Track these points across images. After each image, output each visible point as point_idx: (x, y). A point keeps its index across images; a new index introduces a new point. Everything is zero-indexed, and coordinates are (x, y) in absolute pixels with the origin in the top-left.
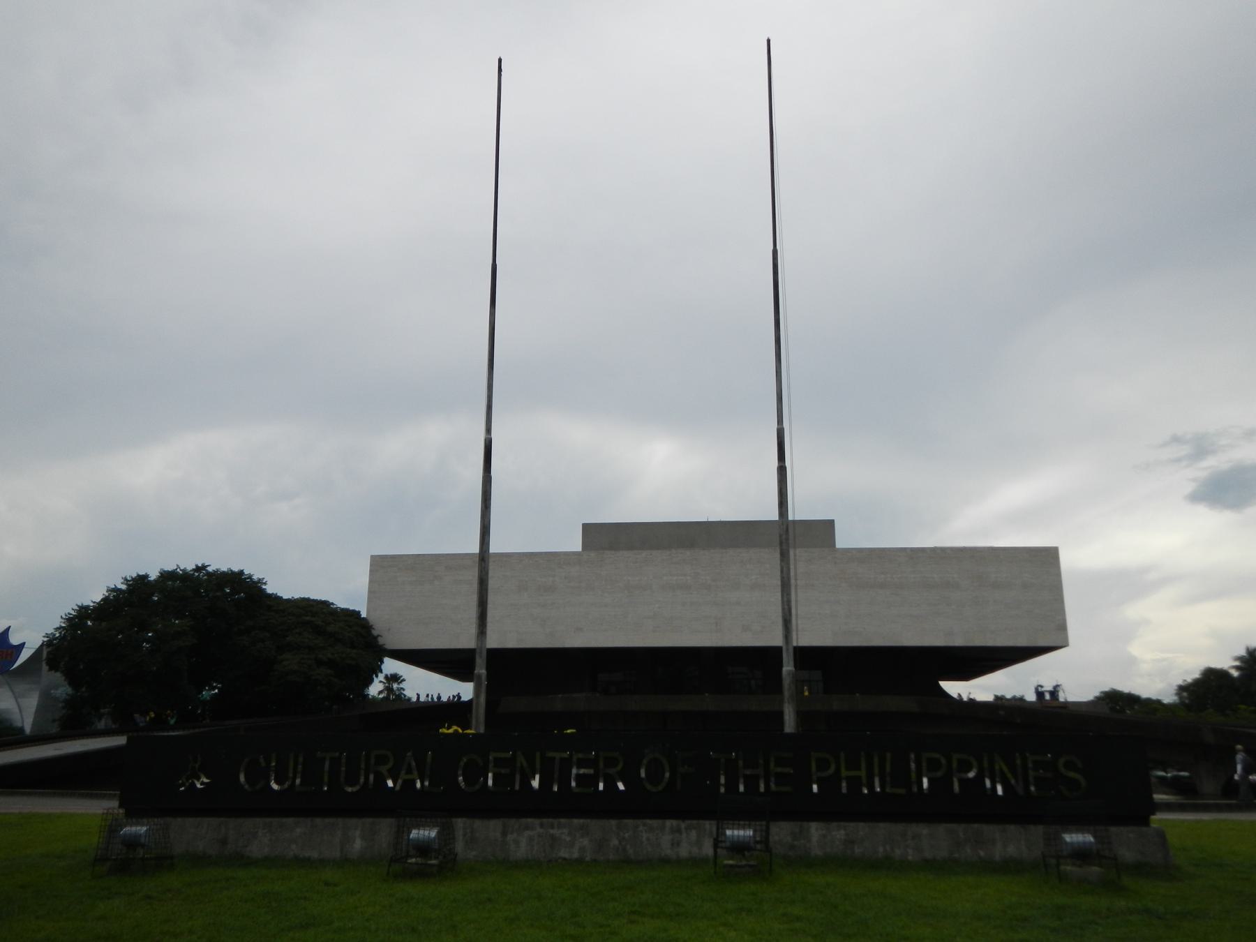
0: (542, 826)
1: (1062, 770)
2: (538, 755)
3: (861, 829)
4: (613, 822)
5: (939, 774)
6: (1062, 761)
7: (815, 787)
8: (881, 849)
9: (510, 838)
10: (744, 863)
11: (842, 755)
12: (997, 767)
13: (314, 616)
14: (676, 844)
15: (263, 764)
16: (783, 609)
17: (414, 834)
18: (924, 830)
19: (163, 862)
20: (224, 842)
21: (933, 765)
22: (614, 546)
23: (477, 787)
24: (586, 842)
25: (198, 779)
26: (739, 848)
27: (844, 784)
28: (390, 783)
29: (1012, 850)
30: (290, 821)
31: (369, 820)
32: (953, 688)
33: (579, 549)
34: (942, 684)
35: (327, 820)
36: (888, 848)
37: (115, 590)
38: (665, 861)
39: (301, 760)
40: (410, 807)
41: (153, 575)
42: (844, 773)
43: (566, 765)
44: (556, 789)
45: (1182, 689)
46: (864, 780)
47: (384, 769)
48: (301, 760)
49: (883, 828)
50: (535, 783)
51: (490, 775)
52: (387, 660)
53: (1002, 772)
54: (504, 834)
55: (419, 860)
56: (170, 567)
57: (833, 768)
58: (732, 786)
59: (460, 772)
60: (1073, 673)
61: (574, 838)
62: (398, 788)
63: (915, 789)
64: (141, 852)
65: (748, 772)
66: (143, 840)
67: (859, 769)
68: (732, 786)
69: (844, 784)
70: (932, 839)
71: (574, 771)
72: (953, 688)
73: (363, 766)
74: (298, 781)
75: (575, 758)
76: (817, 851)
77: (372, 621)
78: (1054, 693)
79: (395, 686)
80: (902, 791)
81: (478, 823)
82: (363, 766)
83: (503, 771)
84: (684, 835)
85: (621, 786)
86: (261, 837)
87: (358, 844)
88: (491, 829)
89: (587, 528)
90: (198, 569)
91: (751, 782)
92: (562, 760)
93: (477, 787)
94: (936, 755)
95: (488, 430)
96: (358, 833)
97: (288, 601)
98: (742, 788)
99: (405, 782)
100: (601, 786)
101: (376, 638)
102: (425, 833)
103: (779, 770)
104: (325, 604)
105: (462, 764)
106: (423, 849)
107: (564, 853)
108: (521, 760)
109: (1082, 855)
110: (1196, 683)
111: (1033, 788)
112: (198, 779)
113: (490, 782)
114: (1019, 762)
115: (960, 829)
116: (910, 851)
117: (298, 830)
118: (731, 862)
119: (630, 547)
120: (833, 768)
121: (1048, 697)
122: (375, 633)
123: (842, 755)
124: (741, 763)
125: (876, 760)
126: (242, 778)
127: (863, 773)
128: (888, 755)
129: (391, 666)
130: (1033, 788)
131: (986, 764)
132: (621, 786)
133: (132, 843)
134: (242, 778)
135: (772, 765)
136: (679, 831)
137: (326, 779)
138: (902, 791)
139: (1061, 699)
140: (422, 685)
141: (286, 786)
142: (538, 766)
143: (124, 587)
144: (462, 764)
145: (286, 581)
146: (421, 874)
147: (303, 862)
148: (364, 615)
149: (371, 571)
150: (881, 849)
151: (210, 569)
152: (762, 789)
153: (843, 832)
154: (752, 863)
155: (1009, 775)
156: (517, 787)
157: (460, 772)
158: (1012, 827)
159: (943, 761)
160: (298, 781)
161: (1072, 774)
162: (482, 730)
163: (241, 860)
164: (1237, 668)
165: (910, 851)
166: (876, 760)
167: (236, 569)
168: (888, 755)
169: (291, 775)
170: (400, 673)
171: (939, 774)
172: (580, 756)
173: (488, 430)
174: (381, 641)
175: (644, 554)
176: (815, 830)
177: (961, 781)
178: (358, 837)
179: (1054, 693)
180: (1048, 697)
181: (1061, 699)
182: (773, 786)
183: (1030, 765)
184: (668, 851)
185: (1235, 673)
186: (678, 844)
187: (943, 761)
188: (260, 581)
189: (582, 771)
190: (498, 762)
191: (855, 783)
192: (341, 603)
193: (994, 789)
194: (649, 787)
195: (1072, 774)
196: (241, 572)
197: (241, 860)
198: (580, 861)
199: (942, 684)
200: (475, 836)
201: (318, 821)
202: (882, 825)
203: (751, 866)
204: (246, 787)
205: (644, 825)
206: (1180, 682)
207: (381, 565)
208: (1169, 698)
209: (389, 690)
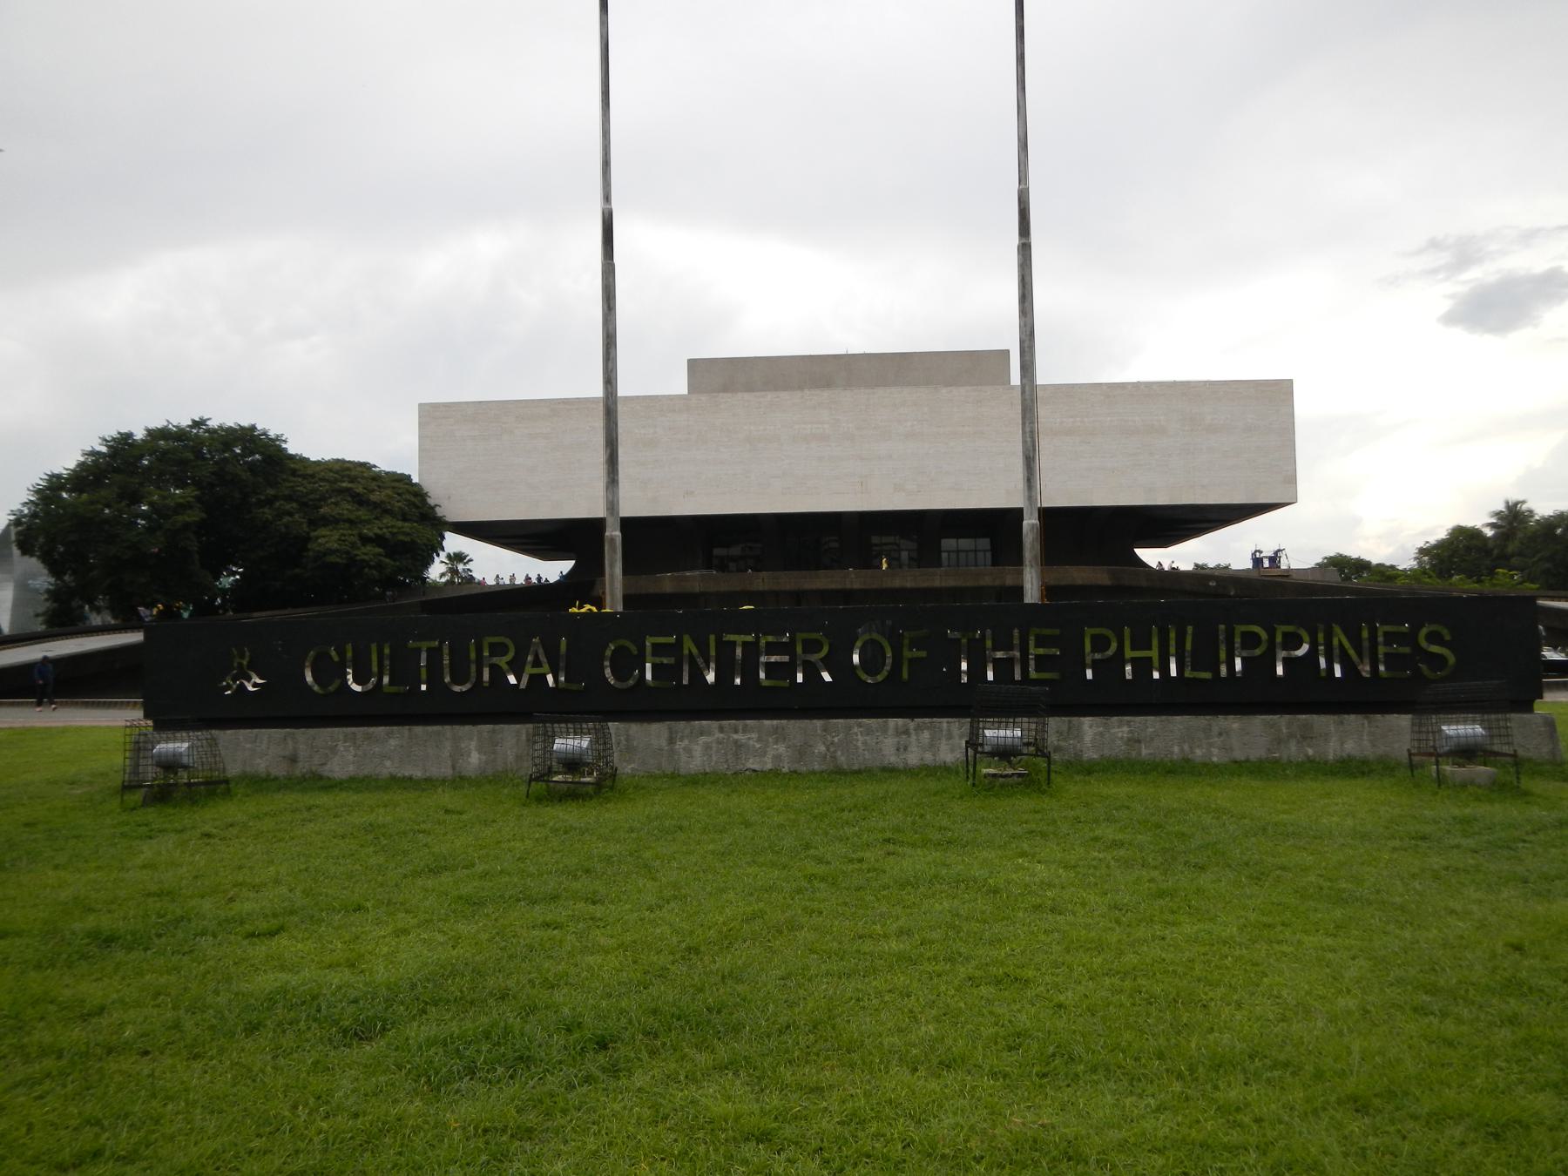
0: (721, 729)
1: (1424, 644)
2: (712, 638)
3: (1150, 724)
4: (818, 723)
5: (1258, 652)
6: (1424, 631)
7: (1089, 674)
8: (1176, 749)
9: (679, 745)
10: (1010, 771)
11: (1127, 630)
12: (1335, 642)
13: (352, 483)
14: (902, 749)
15: (336, 659)
16: (1024, 442)
17: (559, 744)
18: (1233, 723)
19: (216, 787)
20: (293, 760)
21: (1250, 640)
22: (728, 387)
23: (631, 682)
24: (781, 748)
25: (249, 679)
26: (1004, 753)
27: (1128, 668)
28: (512, 680)
29: (1350, 747)
30: (380, 730)
31: (486, 728)
33: (685, 391)
34: (1138, 551)
35: (430, 728)
36: (1186, 747)
37: (93, 453)
38: (890, 771)
39: (387, 651)
40: (532, 708)
41: (139, 435)
42: (1129, 654)
43: (752, 650)
44: (738, 681)
45: (1422, 551)
46: (1156, 662)
47: (502, 661)
48: (387, 651)
49: (1180, 722)
50: (711, 677)
51: (648, 665)
52: (448, 535)
53: (1341, 644)
54: (671, 741)
55: (569, 778)
56: (158, 423)
57: (1114, 645)
58: (977, 672)
59: (607, 663)
60: (1297, 537)
61: (765, 743)
62: (523, 686)
63: (1224, 670)
64: (183, 777)
65: (999, 655)
66: (185, 760)
67: (1149, 648)
68: (977, 672)
69: (1128, 668)
70: (1247, 735)
71: (763, 659)
73: (473, 655)
74: (386, 680)
75: (763, 642)
76: (1090, 754)
77: (427, 487)
78: (1274, 559)
79: (461, 567)
80: (1207, 675)
81: (635, 729)
82: (473, 655)
83: (665, 661)
84: (914, 737)
85: (827, 677)
86: (342, 751)
87: (475, 759)
88: (651, 736)
89: (693, 364)
90: (197, 424)
91: (1003, 668)
92: (745, 644)
93: (631, 682)
94: (1256, 629)
95: (607, 198)
96: (473, 744)
97: (318, 463)
98: (990, 676)
99: (532, 677)
100: (800, 678)
101: (432, 508)
102: (569, 743)
103: (1041, 651)
104: (365, 466)
105: (608, 653)
106: (572, 764)
107: (752, 764)
108: (689, 646)
109: (1467, 753)
110: (1441, 545)
111: (1382, 668)
112: (249, 679)
113: (649, 676)
114: (1365, 634)
115: (1282, 721)
116: (1215, 751)
117: (393, 742)
118: (991, 771)
119: (749, 388)
120: (1114, 645)
121: (1266, 564)
122: (431, 502)
123: (1127, 630)
124: (989, 643)
125: (1173, 635)
126: (309, 678)
127: (1154, 654)
128: (1190, 629)
129: (454, 542)
130: (1382, 668)
131: (1321, 637)
132: (827, 677)
133: (170, 765)
134: (309, 678)
135: (1032, 643)
136: (907, 732)
137: (424, 675)
138: (1207, 675)
139: (1283, 567)
140: (496, 566)
141: (370, 686)
142: (713, 653)
143: (104, 449)
144: (608, 653)
145: (314, 438)
146: (573, 795)
147: (407, 783)
148: (415, 480)
149: (420, 424)
150: (1176, 749)
151: (213, 424)
152: (1018, 677)
153: (1125, 729)
154: (1021, 770)
155: (1352, 652)
156: (685, 682)
157: (607, 663)
158: (1353, 717)
159: (1264, 635)
160: (386, 680)
161: (1435, 649)
162: (620, 609)
163: (318, 782)
164: (1492, 525)
165: (1215, 751)
166: (1173, 635)
167: (245, 423)
168: (1190, 629)
169: (375, 669)
170: (465, 551)
171: (1258, 652)
172: (770, 639)
173: (607, 198)
174: (440, 512)
175: (770, 396)
176: (1089, 726)
177: (1286, 662)
178: (471, 748)
179: (1274, 559)
180: (1266, 564)
181: (1283, 567)
182: (1033, 674)
183: (1381, 639)
184: (892, 759)
185: (1489, 533)
186: (906, 749)
187: (1264, 635)
188: (278, 438)
189: (773, 659)
190: (658, 650)
191: (1143, 667)
193: (1330, 669)
194: (864, 676)
195: (1435, 649)
196: (253, 428)
197: (318, 782)
198: (775, 773)
199: (1138, 551)
200: (642, 743)
201: (418, 730)
202: (1178, 718)
203: (1020, 775)
204: (316, 688)
205: (860, 725)
206: (1421, 544)
207: (433, 416)
208: (1406, 562)
209: (454, 572)
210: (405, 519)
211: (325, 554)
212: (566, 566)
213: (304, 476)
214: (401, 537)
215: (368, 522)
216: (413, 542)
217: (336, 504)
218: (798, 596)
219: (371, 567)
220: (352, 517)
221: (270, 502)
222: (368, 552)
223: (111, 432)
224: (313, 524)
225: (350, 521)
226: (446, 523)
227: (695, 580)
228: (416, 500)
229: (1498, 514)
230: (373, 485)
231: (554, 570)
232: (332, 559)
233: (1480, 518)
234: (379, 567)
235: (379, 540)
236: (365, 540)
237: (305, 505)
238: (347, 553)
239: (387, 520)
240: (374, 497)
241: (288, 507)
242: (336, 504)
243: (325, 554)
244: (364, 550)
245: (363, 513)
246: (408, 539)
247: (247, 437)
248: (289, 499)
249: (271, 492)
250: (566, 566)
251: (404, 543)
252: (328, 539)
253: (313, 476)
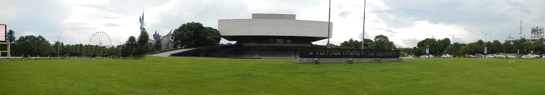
13: (210, 29)
32: (314, 43)
72: (314, 43)
106: (350, 61)
208: (339, 45)
218: (270, 47)
222: (213, 39)
224: (207, 35)
227: (253, 44)
229: (351, 40)
231: (234, 43)
233: (348, 40)
235: (215, 38)
252: (209, 38)
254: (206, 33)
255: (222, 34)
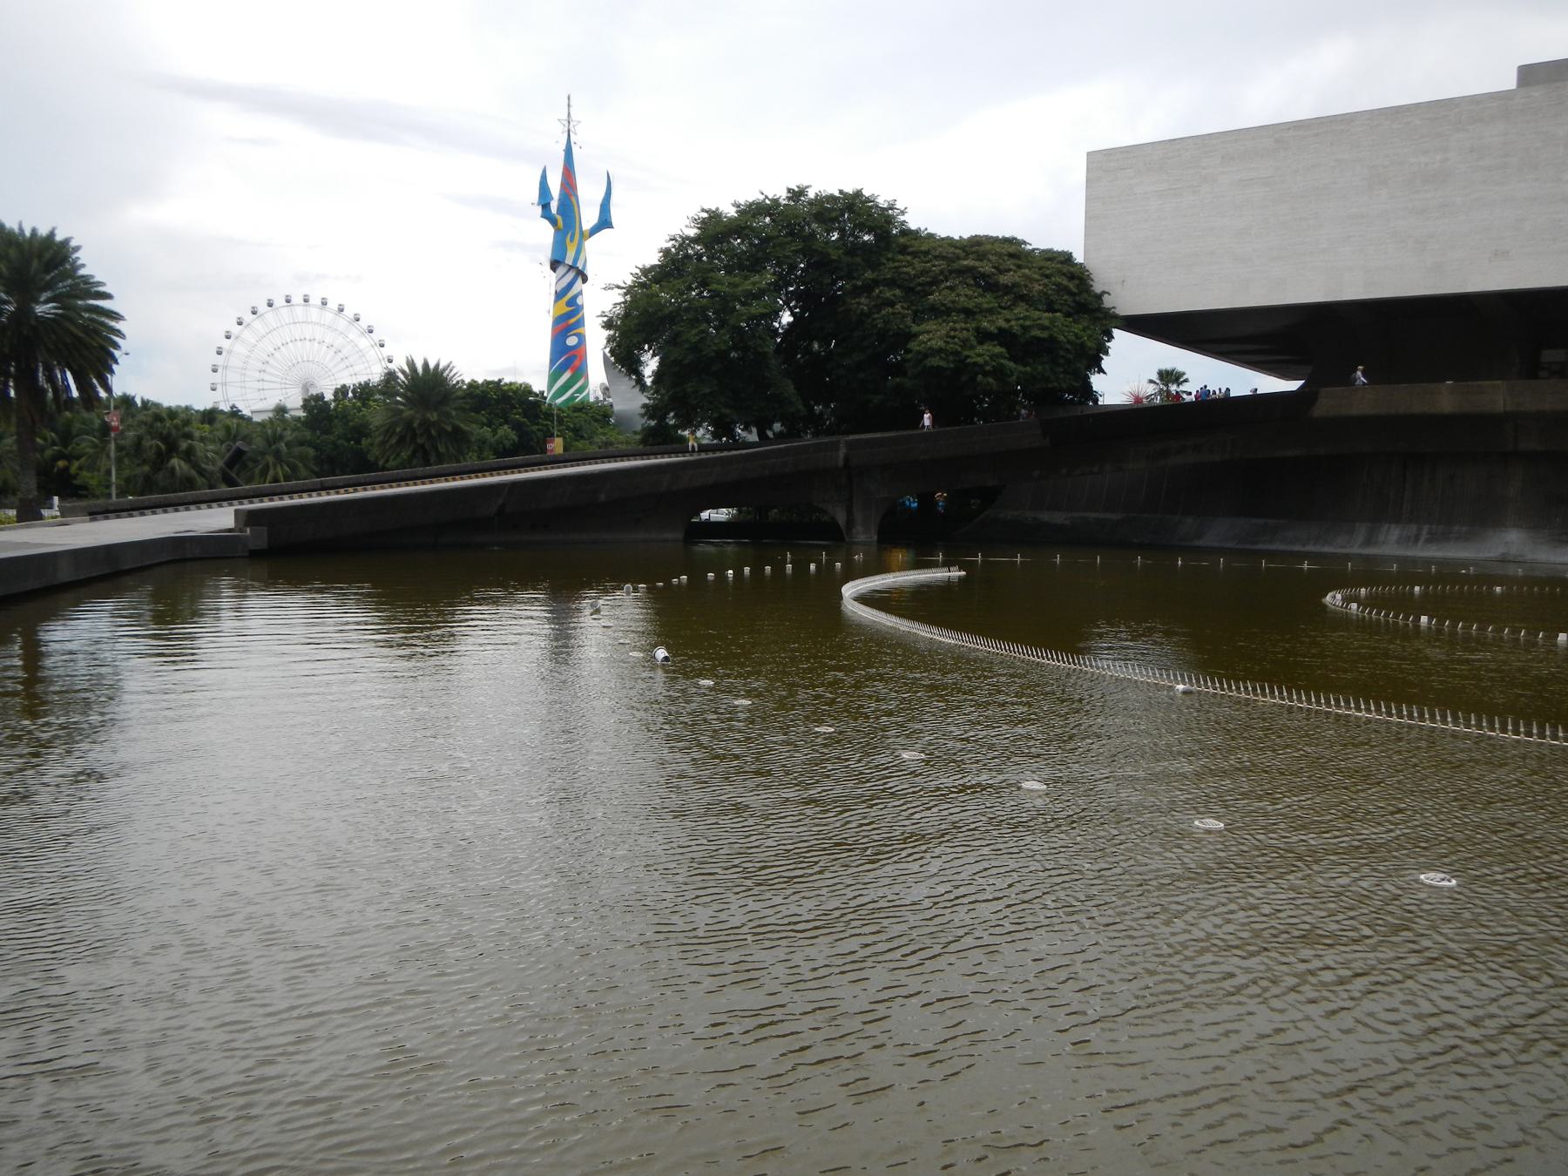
13: (992, 266)
52: (1116, 332)
56: (750, 195)
79: (1173, 388)
90: (797, 194)
122: (1097, 288)
148: (1079, 258)
167: (849, 190)
174: (1108, 302)
192: (1038, 240)
196: (858, 194)
210: (1050, 308)
211: (926, 356)
212: (1300, 383)
213: (915, 254)
214: (1036, 333)
215: (990, 311)
216: (1052, 339)
217: (951, 288)
219: (986, 374)
220: (971, 305)
221: (868, 288)
222: (983, 353)
223: (695, 211)
224: (917, 318)
225: (968, 313)
226: (1116, 317)
228: (1072, 286)
230: (1010, 263)
232: (934, 361)
234: (999, 373)
235: (1003, 337)
236: (984, 336)
237: (911, 290)
238: (957, 353)
239: (1021, 310)
240: (1004, 279)
241: (888, 294)
242: (951, 288)
243: (926, 356)
244: (980, 349)
245: (987, 301)
246: (1045, 335)
247: (854, 210)
248: (891, 283)
249: (869, 275)
250: (1300, 383)
251: (1038, 339)
252: (932, 335)
253: (927, 253)
254: (915, 291)
255: (1126, 302)
